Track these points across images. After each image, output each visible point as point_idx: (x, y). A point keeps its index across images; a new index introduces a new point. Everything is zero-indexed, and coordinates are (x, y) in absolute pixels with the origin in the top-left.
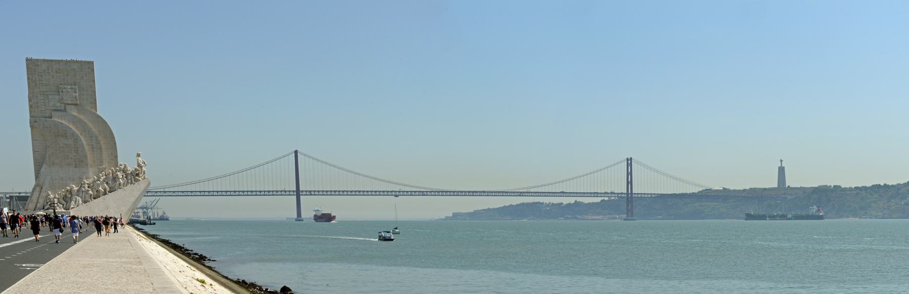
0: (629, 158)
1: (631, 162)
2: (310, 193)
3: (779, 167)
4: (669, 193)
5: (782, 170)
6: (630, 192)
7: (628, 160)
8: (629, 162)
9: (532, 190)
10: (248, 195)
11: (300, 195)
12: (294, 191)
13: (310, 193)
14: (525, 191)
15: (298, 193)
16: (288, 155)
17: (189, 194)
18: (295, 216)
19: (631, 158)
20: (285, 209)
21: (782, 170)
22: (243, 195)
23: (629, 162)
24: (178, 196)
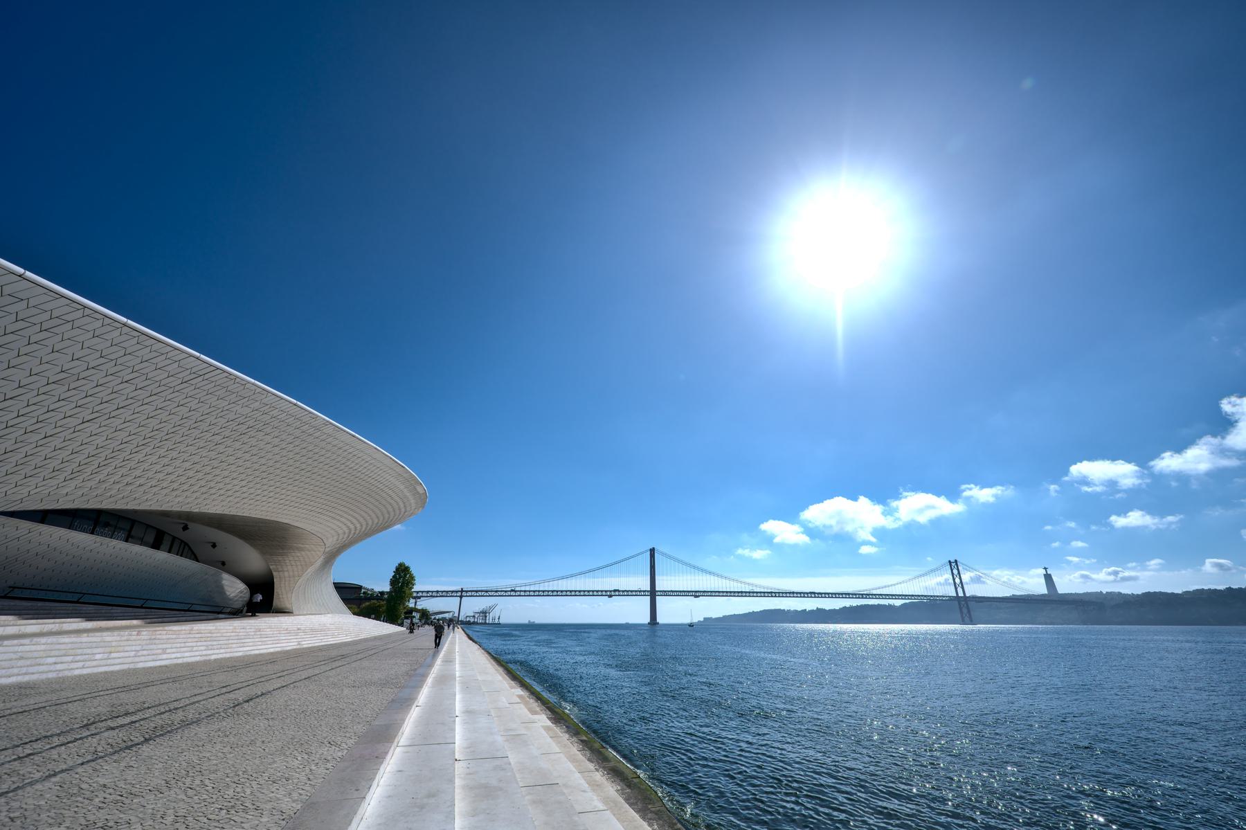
0: (952, 560)
1: (957, 564)
2: (666, 593)
3: (1044, 575)
4: (1000, 596)
5: (1048, 578)
6: (961, 594)
7: (950, 562)
8: (954, 564)
9: (875, 592)
10: (567, 595)
11: (656, 595)
12: (648, 591)
13: (666, 593)
14: (865, 593)
15: (653, 593)
16: (642, 553)
17: (522, 594)
18: (646, 619)
19: (956, 561)
20: (635, 612)
21: (1048, 578)
22: (543, 596)
23: (954, 564)
24: (500, 596)
